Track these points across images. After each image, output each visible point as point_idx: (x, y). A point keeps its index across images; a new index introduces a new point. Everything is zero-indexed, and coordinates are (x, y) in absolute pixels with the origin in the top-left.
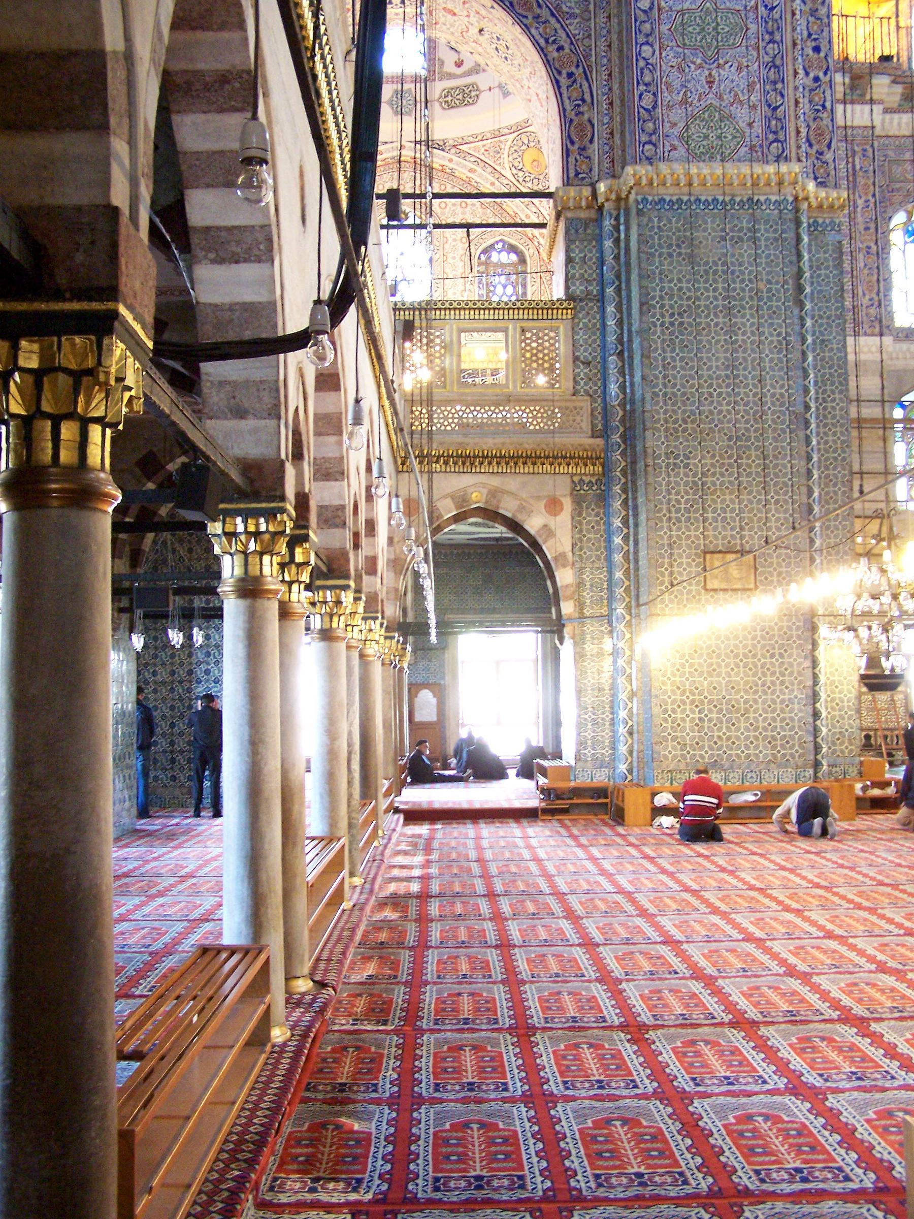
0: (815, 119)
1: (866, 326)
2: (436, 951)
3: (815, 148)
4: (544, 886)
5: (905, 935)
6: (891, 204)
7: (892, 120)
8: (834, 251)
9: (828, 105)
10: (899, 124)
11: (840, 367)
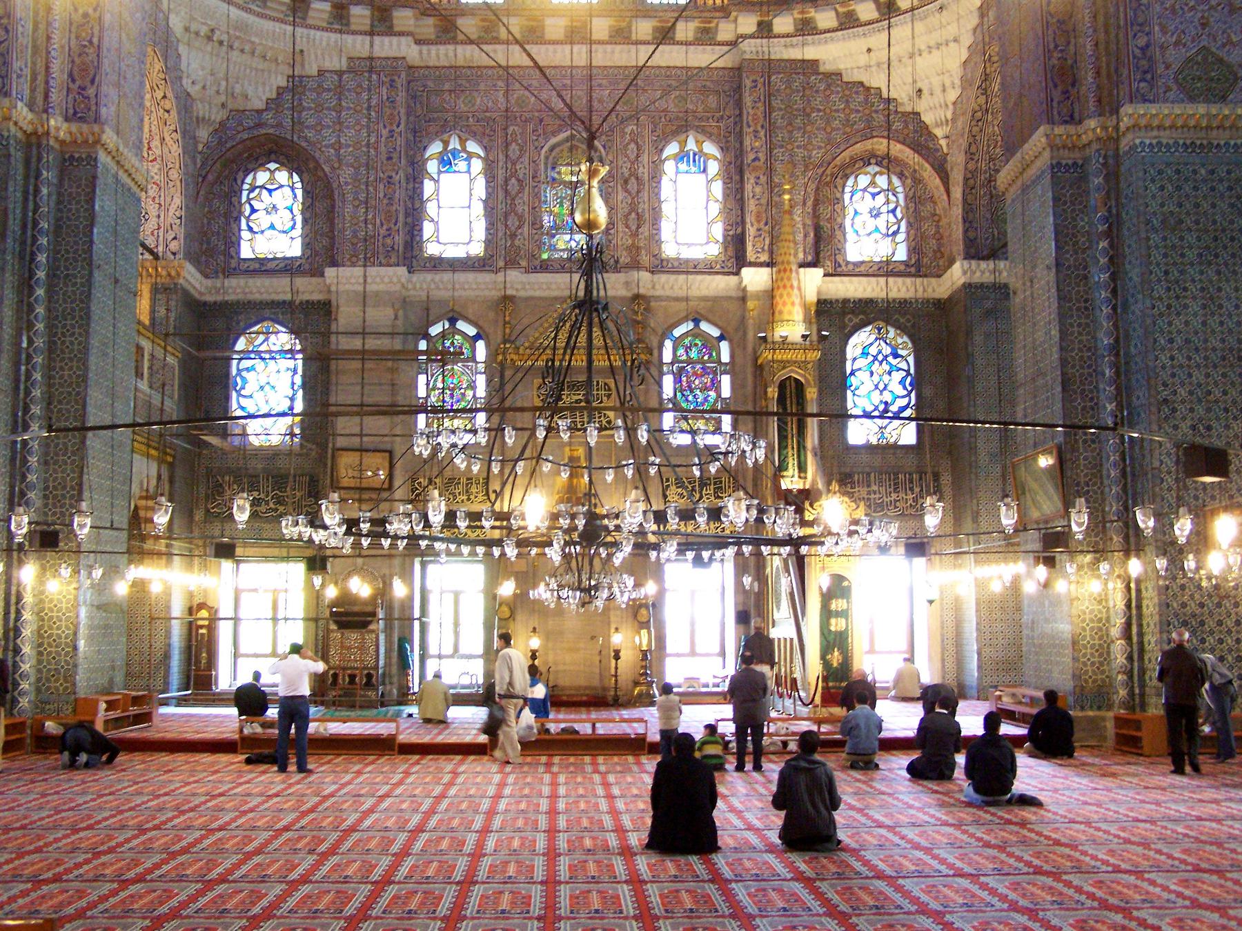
0: (80, 55)
1: (381, 257)
2: (482, 887)
3: (78, 83)
4: (608, 821)
5: (954, 875)
6: (428, 134)
7: (429, 51)
8: (87, 186)
9: (95, 40)
10: (438, 56)
11: (82, 301)
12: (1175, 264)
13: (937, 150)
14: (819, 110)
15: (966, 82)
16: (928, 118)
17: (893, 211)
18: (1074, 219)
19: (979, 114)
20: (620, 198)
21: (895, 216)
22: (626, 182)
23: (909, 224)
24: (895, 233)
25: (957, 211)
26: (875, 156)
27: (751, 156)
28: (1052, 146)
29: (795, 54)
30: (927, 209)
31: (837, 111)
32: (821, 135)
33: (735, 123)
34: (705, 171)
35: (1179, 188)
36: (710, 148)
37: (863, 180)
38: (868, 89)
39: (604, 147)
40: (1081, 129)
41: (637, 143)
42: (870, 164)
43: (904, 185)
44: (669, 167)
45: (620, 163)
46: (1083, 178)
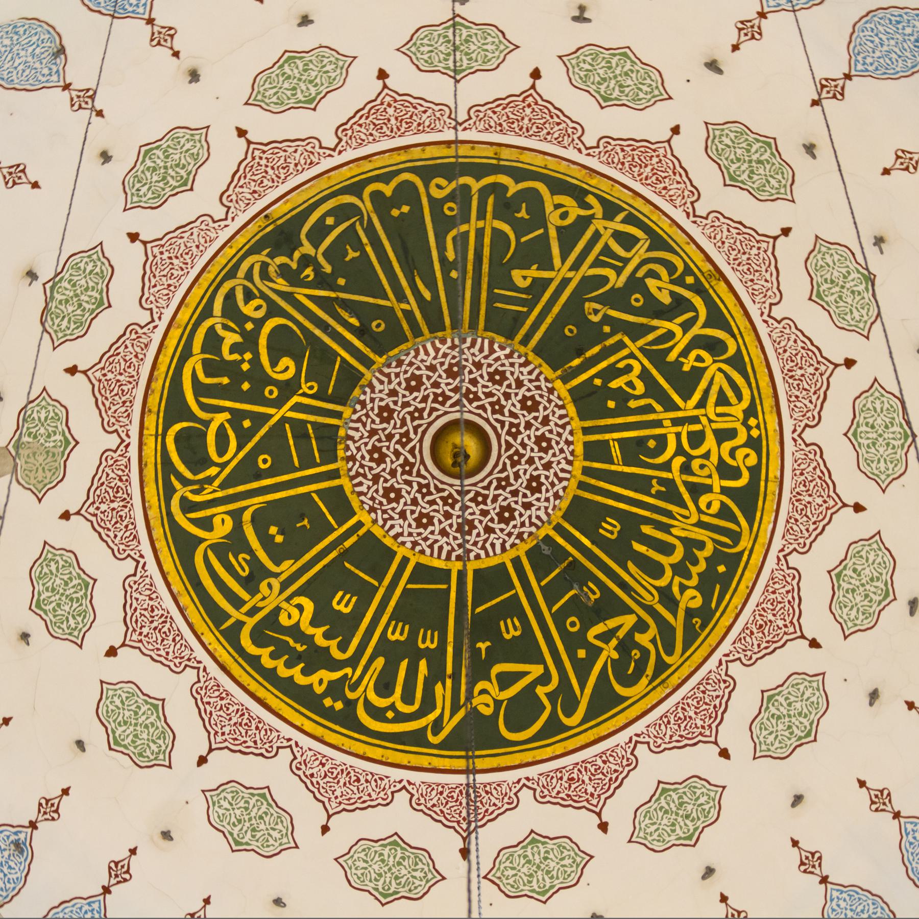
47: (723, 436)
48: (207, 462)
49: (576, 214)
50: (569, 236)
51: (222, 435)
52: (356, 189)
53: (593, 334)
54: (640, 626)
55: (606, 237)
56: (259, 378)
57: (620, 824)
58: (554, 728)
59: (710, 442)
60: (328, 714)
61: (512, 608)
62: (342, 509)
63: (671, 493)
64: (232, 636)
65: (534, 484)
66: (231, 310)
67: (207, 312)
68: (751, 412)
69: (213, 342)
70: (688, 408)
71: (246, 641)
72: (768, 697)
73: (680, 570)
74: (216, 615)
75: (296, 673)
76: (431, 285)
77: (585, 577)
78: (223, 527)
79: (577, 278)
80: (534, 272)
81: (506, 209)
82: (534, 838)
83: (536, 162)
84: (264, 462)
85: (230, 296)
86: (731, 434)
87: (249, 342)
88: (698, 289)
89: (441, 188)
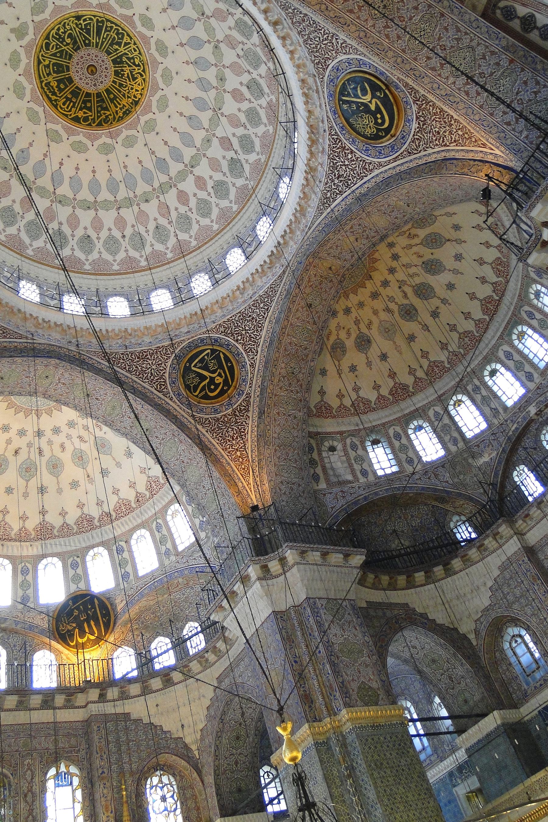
12: (387, 786)
13: (193, 757)
14: (133, 741)
15: (209, 718)
16: (188, 740)
17: (172, 796)
18: (331, 771)
19: (219, 734)
20: (22, 807)
21: (174, 799)
22: (26, 796)
23: (182, 803)
24: (175, 809)
25: (211, 791)
26: (160, 765)
27: (100, 771)
28: (313, 734)
29: (119, 710)
30: (189, 793)
31: (142, 740)
32: (136, 755)
33: (87, 753)
34: (71, 784)
35: (376, 747)
36: (73, 769)
37: (155, 780)
38: (156, 726)
39: (12, 774)
40: (322, 724)
41: (31, 771)
42: (157, 770)
43: (176, 780)
44: (50, 784)
45: (22, 784)
46: (329, 748)
47: (137, 90)
48: (49, 50)
49: (129, 41)
50: (126, 44)
51: (53, 46)
52: (95, 16)
53: (122, 62)
54: (110, 115)
55: (132, 48)
56: (64, 39)
57: (96, 146)
58: (90, 125)
59: (134, 90)
60: (53, 104)
61: (90, 101)
62: (68, 70)
63: (124, 95)
64: (41, 82)
65: (102, 82)
66: (64, 25)
67: (60, 24)
68: (143, 89)
69: (59, 29)
70: (133, 83)
71: (43, 84)
72: (127, 137)
73: (120, 109)
74: (40, 78)
75: (50, 94)
76: (99, 39)
77: (104, 102)
78: (47, 62)
79: (124, 52)
80: (117, 47)
81: (118, 34)
82: (80, 142)
83: (127, 29)
84: (58, 55)
85: (65, 23)
86: (138, 91)
87: (65, 33)
88: (143, 64)
89: (109, 24)
